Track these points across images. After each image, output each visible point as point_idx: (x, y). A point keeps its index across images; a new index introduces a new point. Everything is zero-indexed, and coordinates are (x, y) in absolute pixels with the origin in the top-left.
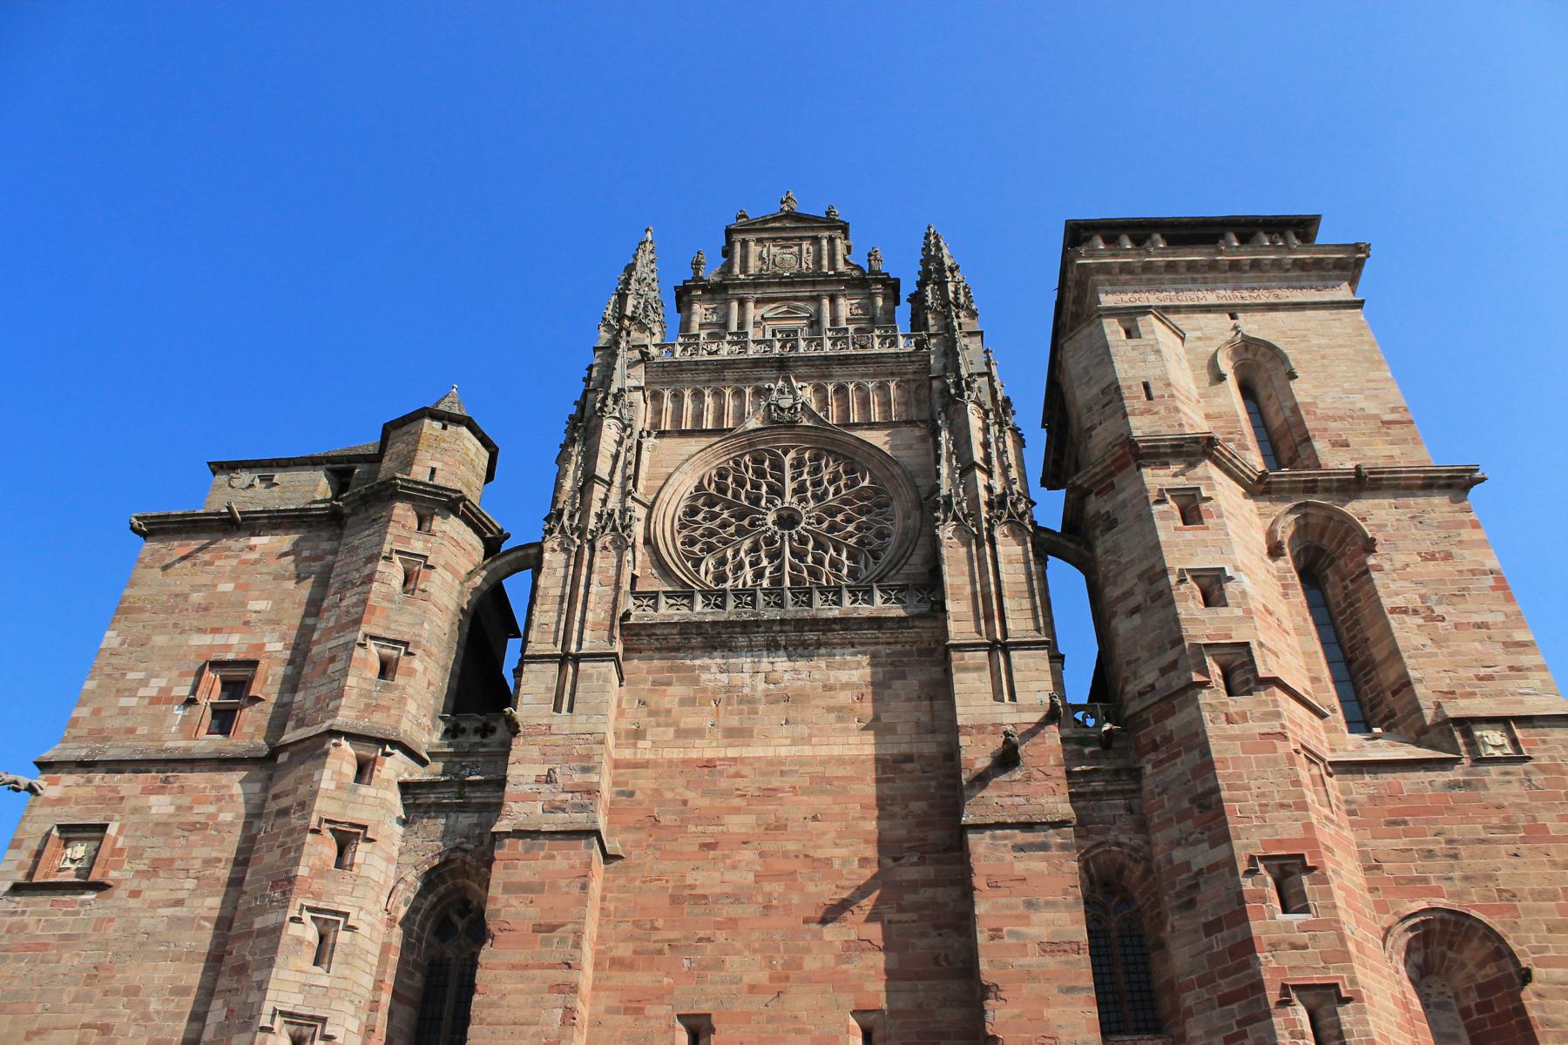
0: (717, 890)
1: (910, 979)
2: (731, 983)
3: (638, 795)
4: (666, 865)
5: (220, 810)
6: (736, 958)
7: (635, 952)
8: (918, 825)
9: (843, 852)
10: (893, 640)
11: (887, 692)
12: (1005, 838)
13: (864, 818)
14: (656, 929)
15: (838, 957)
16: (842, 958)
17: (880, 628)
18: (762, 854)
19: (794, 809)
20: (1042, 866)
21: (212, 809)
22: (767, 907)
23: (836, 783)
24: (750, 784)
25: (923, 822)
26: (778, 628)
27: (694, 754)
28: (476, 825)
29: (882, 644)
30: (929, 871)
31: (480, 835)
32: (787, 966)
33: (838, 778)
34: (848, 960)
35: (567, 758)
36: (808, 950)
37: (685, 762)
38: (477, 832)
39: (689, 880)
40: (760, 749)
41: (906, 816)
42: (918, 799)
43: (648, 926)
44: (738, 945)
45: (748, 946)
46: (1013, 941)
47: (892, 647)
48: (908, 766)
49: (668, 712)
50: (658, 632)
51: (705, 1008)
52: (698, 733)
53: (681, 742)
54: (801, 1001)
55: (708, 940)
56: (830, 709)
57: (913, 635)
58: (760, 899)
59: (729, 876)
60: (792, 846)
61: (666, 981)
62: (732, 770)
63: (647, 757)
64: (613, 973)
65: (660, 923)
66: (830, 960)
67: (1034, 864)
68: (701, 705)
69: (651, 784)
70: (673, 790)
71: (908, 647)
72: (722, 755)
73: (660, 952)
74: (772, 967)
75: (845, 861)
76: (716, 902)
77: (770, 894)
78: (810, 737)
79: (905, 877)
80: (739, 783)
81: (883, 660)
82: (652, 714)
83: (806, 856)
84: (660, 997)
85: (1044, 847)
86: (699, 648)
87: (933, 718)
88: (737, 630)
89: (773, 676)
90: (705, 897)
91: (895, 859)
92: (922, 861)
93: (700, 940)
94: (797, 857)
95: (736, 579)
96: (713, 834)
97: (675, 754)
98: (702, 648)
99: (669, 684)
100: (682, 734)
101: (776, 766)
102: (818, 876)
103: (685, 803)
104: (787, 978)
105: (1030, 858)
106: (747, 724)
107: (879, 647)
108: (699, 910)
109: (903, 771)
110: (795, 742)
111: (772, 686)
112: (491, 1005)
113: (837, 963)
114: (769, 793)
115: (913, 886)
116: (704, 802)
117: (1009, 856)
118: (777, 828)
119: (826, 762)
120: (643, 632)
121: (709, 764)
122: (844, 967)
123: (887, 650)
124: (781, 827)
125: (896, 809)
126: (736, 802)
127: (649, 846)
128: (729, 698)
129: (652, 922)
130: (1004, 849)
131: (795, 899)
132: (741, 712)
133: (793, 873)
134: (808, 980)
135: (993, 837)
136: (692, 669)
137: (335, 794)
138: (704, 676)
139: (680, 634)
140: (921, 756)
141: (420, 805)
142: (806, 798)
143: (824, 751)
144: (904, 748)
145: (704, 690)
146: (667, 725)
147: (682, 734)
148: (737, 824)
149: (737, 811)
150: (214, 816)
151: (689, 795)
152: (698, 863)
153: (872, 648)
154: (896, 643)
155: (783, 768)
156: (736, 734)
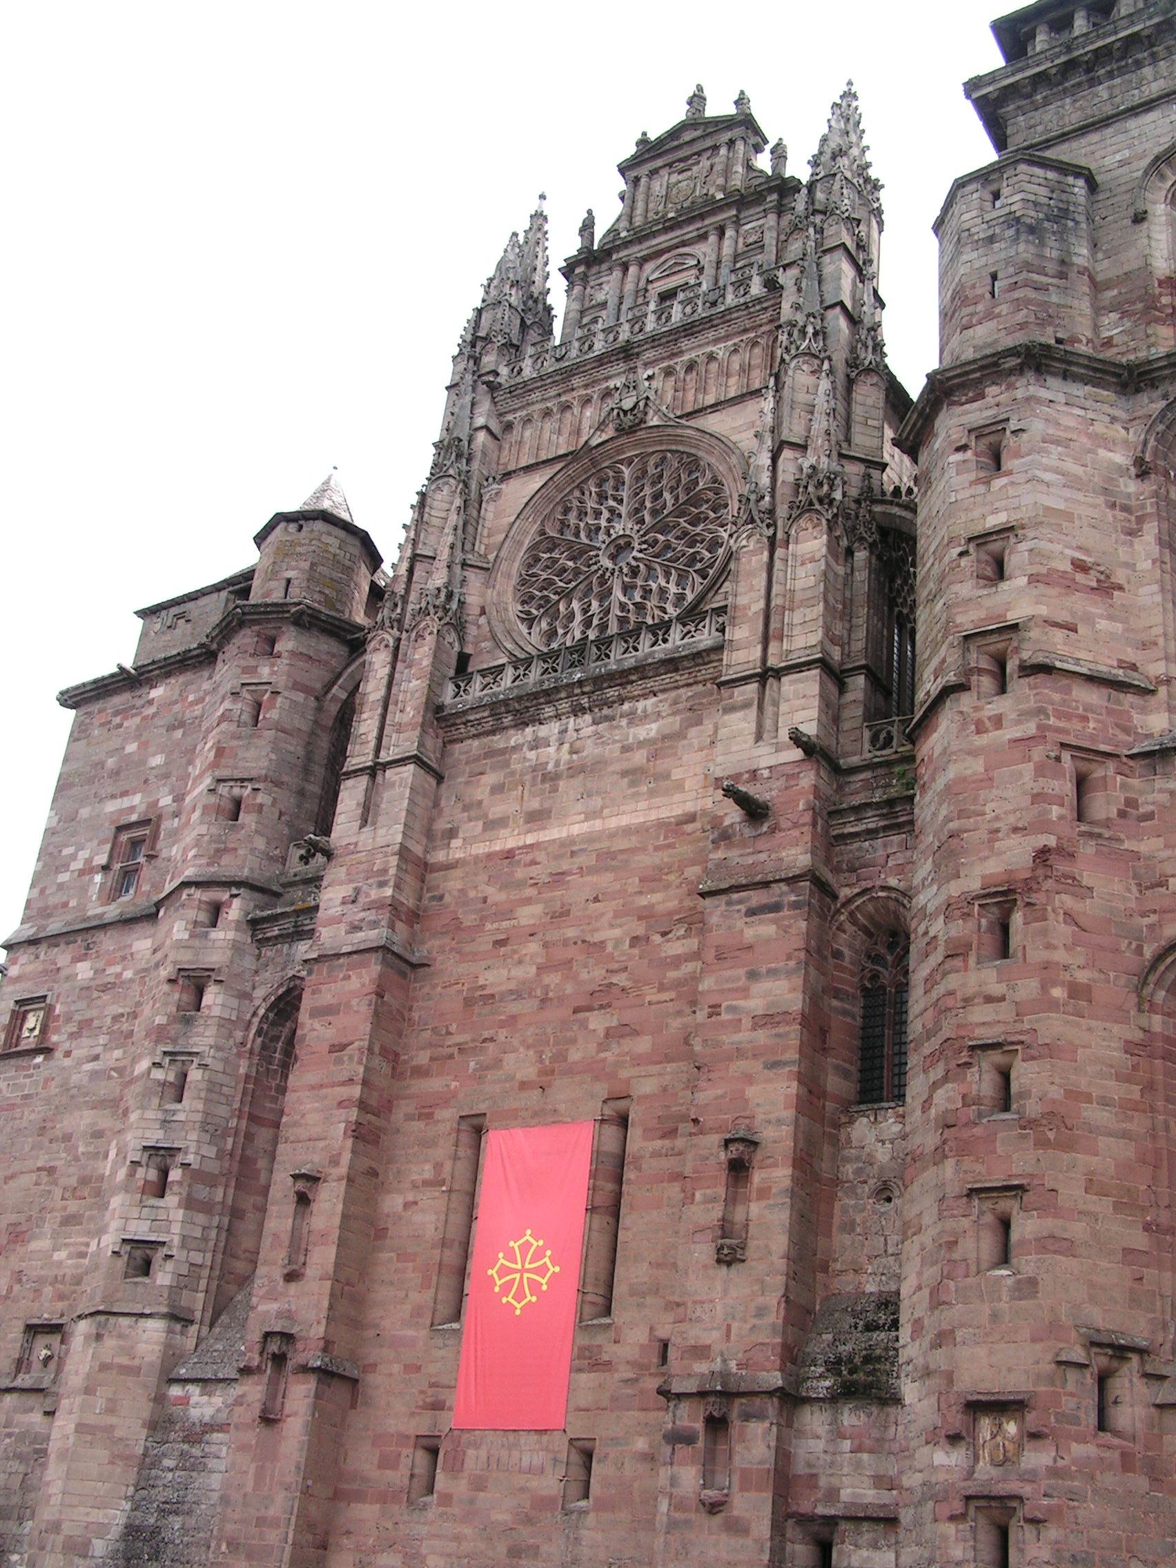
0: (504, 988)
1: (661, 1062)
2: (506, 1081)
3: (447, 898)
4: (463, 968)
5: (124, 969)
6: (512, 1056)
7: (431, 1059)
9: (617, 932)
10: (691, 681)
12: (740, 902)
13: (641, 893)
14: (449, 1033)
15: (600, 1044)
16: (602, 1047)
17: (676, 670)
18: (546, 945)
19: (577, 892)
21: (118, 969)
22: (544, 1000)
23: (620, 857)
26: (577, 691)
27: (497, 847)
29: (683, 686)
32: (554, 1058)
33: (622, 851)
35: (369, 874)
36: (573, 1041)
37: (489, 856)
39: (481, 982)
40: (556, 830)
41: (678, 887)
42: (693, 863)
43: (444, 1032)
44: (516, 1042)
45: (523, 1042)
47: (694, 687)
48: (689, 828)
49: (480, 802)
50: (471, 718)
51: (482, 1108)
55: (492, 1040)
57: (711, 670)
58: (539, 993)
60: (571, 933)
62: (528, 858)
63: (457, 856)
64: (413, 1082)
65: (453, 1028)
66: (592, 1047)
68: (509, 790)
69: (458, 885)
71: (709, 685)
72: (521, 844)
73: (451, 1057)
74: (541, 1061)
75: (618, 942)
76: (500, 1001)
77: (548, 986)
78: (602, 808)
79: (671, 952)
80: (534, 871)
81: (681, 706)
82: (466, 808)
83: (584, 941)
84: (446, 1099)
85: (775, 908)
86: (512, 727)
88: (542, 700)
90: (493, 996)
91: (664, 934)
93: (485, 1041)
94: (575, 943)
97: (480, 849)
98: (515, 726)
101: (568, 848)
102: (591, 961)
103: (485, 900)
104: (552, 1072)
105: (761, 922)
106: (546, 805)
107: (682, 691)
108: (486, 1010)
110: (590, 816)
111: (575, 756)
113: (599, 1051)
114: (558, 878)
115: (677, 961)
116: (502, 897)
117: (739, 924)
118: (562, 915)
119: (612, 835)
120: (458, 721)
121: (509, 855)
122: (602, 1055)
123: (685, 693)
126: (530, 892)
127: (452, 949)
128: (534, 778)
129: (447, 1027)
130: (737, 915)
131: (569, 989)
132: (543, 792)
133: (570, 961)
134: (570, 1072)
135: (729, 903)
136: (503, 751)
137: (191, 943)
139: (492, 716)
141: (268, 939)
142: (589, 878)
143: (613, 823)
144: (690, 807)
145: (512, 774)
146: (477, 819)
147: (492, 825)
148: (528, 915)
149: (528, 901)
150: (119, 975)
152: (490, 962)
153: (673, 694)
154: (696, 683)
155: (575, 848)
156: (536, 818)
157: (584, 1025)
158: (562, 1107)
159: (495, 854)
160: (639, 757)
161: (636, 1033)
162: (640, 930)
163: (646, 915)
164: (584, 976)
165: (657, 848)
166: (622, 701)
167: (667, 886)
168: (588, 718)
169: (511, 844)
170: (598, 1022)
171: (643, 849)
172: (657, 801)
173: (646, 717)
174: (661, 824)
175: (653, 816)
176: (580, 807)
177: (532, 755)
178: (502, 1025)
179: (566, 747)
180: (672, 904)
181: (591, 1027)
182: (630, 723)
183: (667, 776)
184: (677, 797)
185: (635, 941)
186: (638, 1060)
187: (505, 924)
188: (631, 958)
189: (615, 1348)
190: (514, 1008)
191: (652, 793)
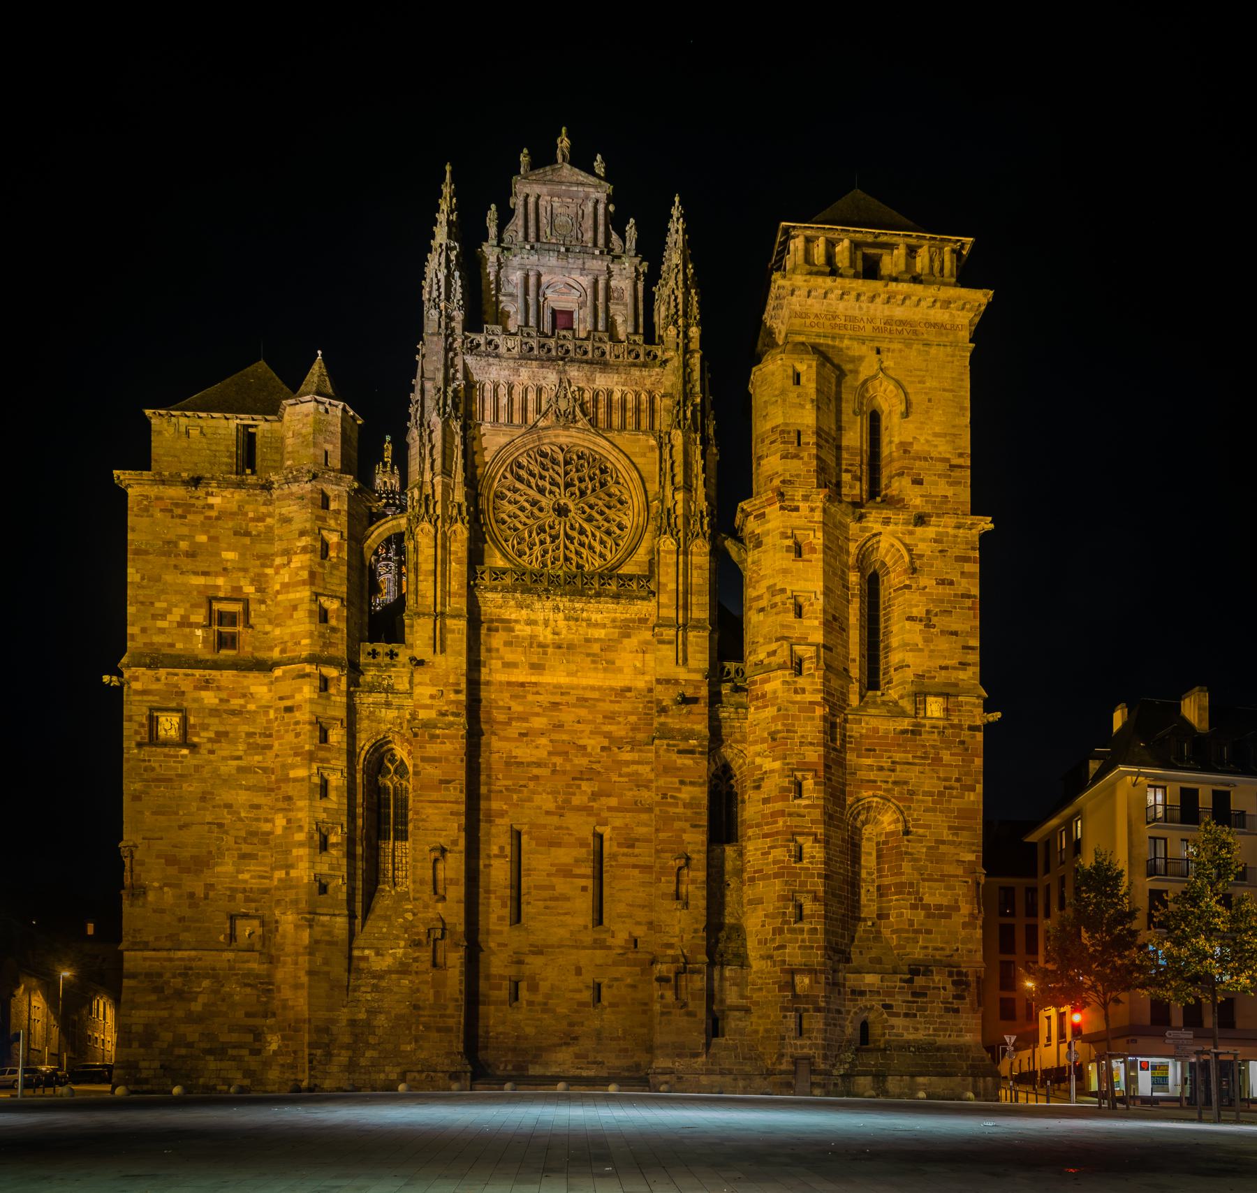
0: (529, 760)
8: (633, 729)
9: (592, 742)
11: (620, 646)
16: (590, 800)
18: (551, 741)
19: (567, 716)
20: (691, 762)
22: (554, 772)
24: (544, 699)
25: (634, 728)
27: (513, 679)
28: (398, 717)
30: (634, 756)
31: (401, 723)
32: (564, 801)
34: (594, 800)
36: (574, 794)
37: (509, 684)
38: (399, 721)
42: (632, 714)
44: (540, 789)
45: (544, 791)
46: (672, 801)
48: (628, 694)
49: (498, 650)
52: (514, 665)
53: (506, 669)
54: (572, 820)
55: (525, 786)
56: (588, 655)
59: (535, 752)
60: (565, 737)
61: (505, 807)
62: (535, 690)
65: (500, 776)
66: (585, 799)
67: (687, 761)
70: (503, 700)
72: (528, 680)
73: (501, 791)
74: (556, 802)
78: (577, 671)
80: (539, 698)
81: (618, 624)
87: (644, 666)
89: (557, 630)
90: (522, 763)
91: (619, 748)
92: (632, 750)
93: (521, 786)
95: (530, 555)
96: (525, 728)
99: (497, 630)
100: (508, 665)
103: (509, 708)
104: (564, 808)
109: (625, 697)
110: (569, 674)
111: (556, 637)
112: (423, 820)
114: (555, 705)
115: (627, 763)
118: (559, 726)
119: (584, 688)
121: (522, 685)
122: (591, 804)
124: (559, 726)
125: (621, 719)
126: (537, 710)
136: (509, 621)
138: (517, 627)
140: (636, 689)
143: (584, 682)
144: (627, 683)
145: (517, 637)
148: (539, 723)
149: (537, 715)
151: (512, 704)
152: (518, 744)
156: (536, 667)
157: (579, 787)
158: (571, 826)
159: (514, 683)
160: (596, 648)
161: (609, 796)
162: (606, 743)
163: (607, 735)
164: (576, 761)
165: (611, 702)
166: (583, 610)
167: (619, 723)
168: (561, 614)
169: (522, 679)
170: (585, 786)
171: (604, 701)
172: (609, 675)
173: (596, 625)
174: (612, 689)
175: (607, 683)
176: (562, 667)
177: (528, 629)
178: (530, 779)
179: (549, 628)
180: (623, 733)
181: (584, 788)
182: (589, 625)
183: (613, 663)
184: (619, 676)
185: (603, 749)
186: (610, 809)
187: (525, 725)
188: (602, 757)
189: (613, 940)
190: (536, 771)
191: (605, 670)
